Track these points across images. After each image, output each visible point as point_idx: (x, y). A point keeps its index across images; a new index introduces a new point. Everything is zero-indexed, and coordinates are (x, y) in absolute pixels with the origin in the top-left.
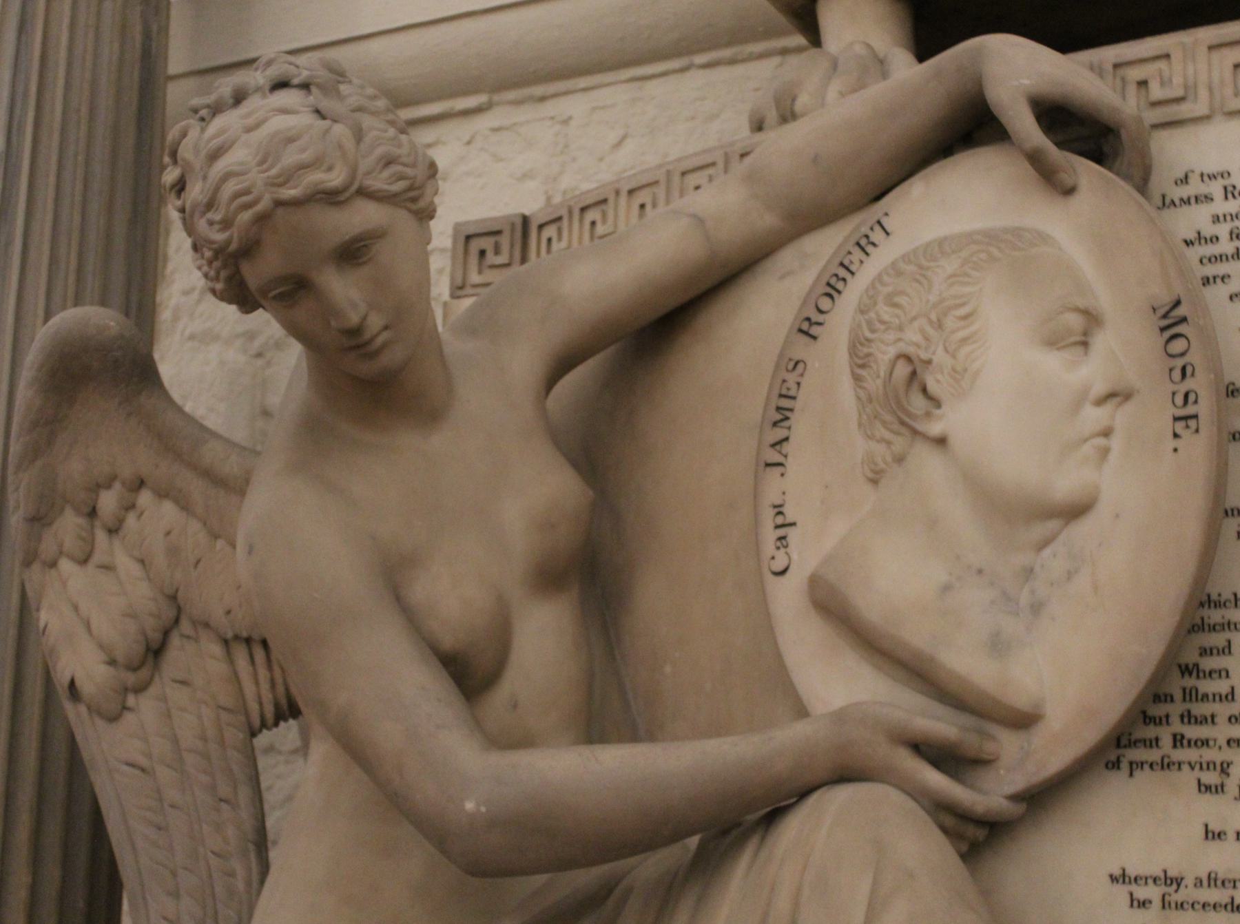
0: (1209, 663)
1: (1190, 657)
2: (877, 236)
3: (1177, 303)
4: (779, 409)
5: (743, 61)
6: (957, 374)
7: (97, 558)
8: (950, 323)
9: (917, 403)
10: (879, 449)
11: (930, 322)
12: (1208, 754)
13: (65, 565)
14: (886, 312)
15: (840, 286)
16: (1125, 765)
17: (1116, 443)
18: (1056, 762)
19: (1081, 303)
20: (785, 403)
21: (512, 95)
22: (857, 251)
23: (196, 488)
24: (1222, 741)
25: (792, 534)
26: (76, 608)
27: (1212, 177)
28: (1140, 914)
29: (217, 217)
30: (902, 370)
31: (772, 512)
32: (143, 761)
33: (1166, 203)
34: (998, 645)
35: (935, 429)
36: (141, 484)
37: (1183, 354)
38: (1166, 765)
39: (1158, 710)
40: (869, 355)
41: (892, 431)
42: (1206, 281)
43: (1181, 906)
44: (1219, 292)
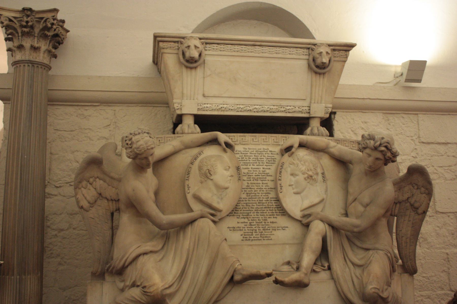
2: (202, 153)
3: (239, 167)
4: (188, 173)
5: (147, 106)
6: (215, 172)
10: (202, 179)
11: (211, 166)
13: (82, 189)
15: (197, 159)
16: (229, 216)
19: (229, 166)
20: (189, 172)
21: (104, 104)
23: (108, 179)
25: (190, 188)
26: (83, 195)
27: (239, 151)
28: (231, 231)
31: (187, 185)
32: (93, 217)
34: (218, 203)
35: (211, 178)
37: (239, 172)
38: (233, 215)
40: (202, 168)
41: (204, 177)
43: (235, 230)
44: (241, 164)
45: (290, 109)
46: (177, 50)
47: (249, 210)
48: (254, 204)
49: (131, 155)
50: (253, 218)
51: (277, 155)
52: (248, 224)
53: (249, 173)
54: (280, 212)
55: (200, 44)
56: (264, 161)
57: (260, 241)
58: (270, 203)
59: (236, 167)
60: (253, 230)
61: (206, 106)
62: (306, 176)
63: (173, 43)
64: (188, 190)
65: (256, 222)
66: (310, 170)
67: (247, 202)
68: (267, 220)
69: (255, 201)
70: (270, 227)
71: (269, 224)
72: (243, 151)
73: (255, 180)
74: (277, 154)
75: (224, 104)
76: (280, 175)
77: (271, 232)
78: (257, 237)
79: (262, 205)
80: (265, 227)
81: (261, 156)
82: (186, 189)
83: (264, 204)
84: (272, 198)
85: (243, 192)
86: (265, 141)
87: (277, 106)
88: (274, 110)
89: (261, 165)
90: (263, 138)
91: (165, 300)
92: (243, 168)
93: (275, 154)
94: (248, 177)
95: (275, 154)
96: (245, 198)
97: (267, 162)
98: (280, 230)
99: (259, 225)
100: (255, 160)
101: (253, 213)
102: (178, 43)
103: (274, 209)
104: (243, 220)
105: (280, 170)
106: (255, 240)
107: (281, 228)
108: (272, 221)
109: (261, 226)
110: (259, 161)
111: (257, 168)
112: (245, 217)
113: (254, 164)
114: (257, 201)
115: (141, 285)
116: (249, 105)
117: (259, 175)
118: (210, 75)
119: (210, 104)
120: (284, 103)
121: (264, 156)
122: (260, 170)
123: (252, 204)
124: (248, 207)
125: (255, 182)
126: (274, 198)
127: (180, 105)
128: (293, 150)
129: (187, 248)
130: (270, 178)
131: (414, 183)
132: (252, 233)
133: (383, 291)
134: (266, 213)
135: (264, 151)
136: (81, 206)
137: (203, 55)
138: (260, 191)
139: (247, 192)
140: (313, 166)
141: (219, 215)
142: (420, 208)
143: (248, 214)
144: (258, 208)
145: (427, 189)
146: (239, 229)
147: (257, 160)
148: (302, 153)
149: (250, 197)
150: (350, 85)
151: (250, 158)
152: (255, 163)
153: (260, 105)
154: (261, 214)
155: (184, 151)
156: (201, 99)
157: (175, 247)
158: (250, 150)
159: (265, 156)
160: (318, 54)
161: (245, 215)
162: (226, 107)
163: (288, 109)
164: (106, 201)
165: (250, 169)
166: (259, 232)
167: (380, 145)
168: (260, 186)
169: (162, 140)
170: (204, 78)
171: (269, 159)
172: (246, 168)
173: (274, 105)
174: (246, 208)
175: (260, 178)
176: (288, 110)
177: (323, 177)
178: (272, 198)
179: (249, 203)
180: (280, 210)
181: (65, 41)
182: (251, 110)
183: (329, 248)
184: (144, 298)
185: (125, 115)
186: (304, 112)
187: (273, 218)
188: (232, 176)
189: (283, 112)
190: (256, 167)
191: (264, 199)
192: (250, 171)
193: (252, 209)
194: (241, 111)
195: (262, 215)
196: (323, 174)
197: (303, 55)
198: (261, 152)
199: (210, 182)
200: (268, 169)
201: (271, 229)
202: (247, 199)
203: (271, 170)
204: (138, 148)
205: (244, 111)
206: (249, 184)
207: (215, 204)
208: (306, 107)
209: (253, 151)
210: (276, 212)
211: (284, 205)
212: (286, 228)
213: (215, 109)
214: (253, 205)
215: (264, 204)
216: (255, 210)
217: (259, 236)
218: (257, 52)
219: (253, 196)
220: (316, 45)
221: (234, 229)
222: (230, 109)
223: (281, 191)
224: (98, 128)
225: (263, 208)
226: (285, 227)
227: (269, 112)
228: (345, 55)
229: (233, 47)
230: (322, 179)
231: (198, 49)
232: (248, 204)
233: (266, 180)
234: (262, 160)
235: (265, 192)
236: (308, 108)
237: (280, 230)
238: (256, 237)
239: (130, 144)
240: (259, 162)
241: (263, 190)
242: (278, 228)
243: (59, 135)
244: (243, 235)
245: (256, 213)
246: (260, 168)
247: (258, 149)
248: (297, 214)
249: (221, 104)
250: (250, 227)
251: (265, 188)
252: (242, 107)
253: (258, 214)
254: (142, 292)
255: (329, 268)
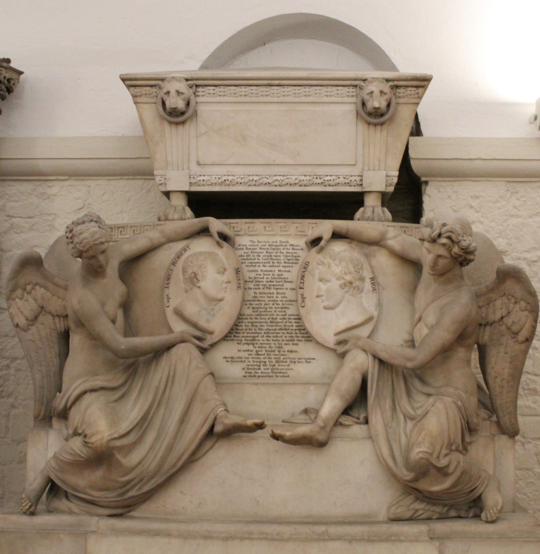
0: (239, 324)
1: (237, 323)
2: (187, 249)
3: (239, 268)
4: (168, 277)
7: (25, 298)
8: (202, 268)
9: (195, 280)
12: (239, 338)
13: (17, 300)
14: (189, 263)
15: (180, 257)
16: (226, 340)
17: (228, 290)
18: (217, 339)
20: (169, 277)
21: (75, 178)
22: (183, 251)
23: (51, 286)
24: (241, 336)
26: (19, 309)
27: (244, 246)
29: (82, 245)
30: (193, 275)
31: (166, 296)
33: (237, 249)
34: (208, 321)
35: (198, 285)
36: (37, 284)
37: (239, 277)
38: (232, 340)
39: (232, 331)
42: (242, 263)
43: (234, 362)
44: (244, 265)
45: (330, 180)
46: (155, 98)
47: (256, 333)
48: (263, 324)
49: (73, 253)
50: (262, 344)
51: (303, 251)
52: (254, 352)
53: (257, 278)
54: (303, 337)
55: (186, 88)
56: (280, 260)
57: (272, 378)
58: (288, 322)
59: (235, 269)
60: (260, 362)
61: (201, 178)
62: (342, 281)
63: (149, 88)
64: (167, 302)
65: (266, 351)
66: (348, 274)
67: (254, 320)
68: (282, 348)
69: (265, 319)
70: (287, 358)
71: (286, 353)
72: (249, 245)
73: (265, 288)
74: (302, 249)
75: (228, 176)
76: (302, 281)
77: (289, 365)
78: (266, 373)
79: (276, 326)
80: (280, 358)
81: (277, 253)
82: (166, 300)
83: (279, 324)
84: (292, 315)
85: (248, 306)
86: (283, 229)
87: (310, 176)
88: (305, 182)
89: (276, 266)
90: (281, 224)
91: (113, 455)
92: (248, 270)
93: (298, 249)
94: (255, 284)
95: (298, 249)
96: (250, 315)
97: (285, 261)
98: (303, 362)
99: (270, 355)
100: (266, 258)
101: (261, 337)
102: (156, 88)
103: (293, 331)
104: (246, 347)
105: (302, 274)
106: (262, 376)
107: (304, 361)
108: (290, 350)
109: (273, 357)
110: (272, 261)
111: (269, 271)
112: (249, 342)
113: (265, 265)
114: (269, 319)
115: (83, 432)
116: (267, 175)
117: (272, 280)
118: (206, 132)
119: (208, 175)
120: (320, 171)
121: (281, 253)
122: (273, 273)
123: (260, 324)
124: (255, 328)
125: (267, 291)
126: (295, 315)
127: (163, 179)
128: (322, 243)
129: (157, 384)
130: (287, 285)
131: (509, 295)
132: (260, 366)
133: (438, 457)
134: (282, 337)
135: (282, 245)
136: (16, 323)
137: (192, 103)
138: (273, 304)
139: (254, 306)
140: (354, 267)
141: (210, 339)
142: (520, 334)
143: (254, 338)
144: (270, 330)
145: (528, 303)
146: (240, 360)
147: (271, 258)
148: (339, 247)
149: (258, 313)
150: (449, 139)
151: (260, 256)
152: (267, 263)
153: (283, 176)
154: (274, 339)
155: (166, 246)
156: (195, 169)
157: (143, 382)
158: (260, 244)
159: (283, 253)
160: (368, 94)
161: (250, 340)
162: (231, 180)
163: (328, 181)
164: (51, 317)
165: (260, 272)
166: (270, 365)
167: (440, 235)
168: (273, 297)
169: (137, 231)
170: (197, 137)
171: (288, 256)
172: (253, 271)
173: (305, 175)
174: (251, 330)
175: (274, 285)
176: (327, 181)
177: (373, 284)
178: (292, 315)
179: (256, 322)
180: (303, 333)
181: (16, 87)
182: (269, 183)
183: (369, 391)
184: (84, 451)
185: (105, 193)
186: (353, 184)
187: (293, 344)
188: (228, 282)
189: (320, 185)
190: (268, 268)
191: (279, 317)
192: (259, 275)
193: (260, 331)
194: (255, 185)
195: (276, 340)
196: (372, 279)
197: (348, 96)
198: (276, 246)
199: (197, 291)
200: (287, 271)
201: (288, 360)
202: (253, 317)
203: (293, 273)
204: (80, 243)
205: (259, 184)
206: (257, 294)
207: (203, 323)
208: (357, 177)
209: (265, 245)
210: (297, 337)
211: (308, 326)
212: (312, 361)
213: (216, 183)
214: (261, 326)
215: (279, 324)
216: (265, 333)
217: (270, 371)
218: (275, 95)
219: (263, 311)
220: (366, 80)
221: (232, 360)
222: (238, 183)
223: (303, 305)
224: (67, 213)
225: (277, 329)
226: (311, 359)
227: (297, 185)
228: (417, 94)
229: (238, 89)
230: (371, 287)
231: (183, 96)
232: (254, 324)
233: (283, 289)
234: (278, 258)
235: (281, 306)
236: (360, 178)
237: (303, 362)
238: (264, 373)
239: (71, 238)
240: (274, 261)
241: (277, 302)
242: (300, 360)
243: (12, 223)
244: (246, 370)
245: (266, 337)
246: (274, 271)
247: (272, 242)
248: (330, 340)
249: (225, 175)
250: (256, 358)
251: (281, 301)
252: (256, 178)
253: (269, 339)
254: (83, 443)
255: (366, 422)
